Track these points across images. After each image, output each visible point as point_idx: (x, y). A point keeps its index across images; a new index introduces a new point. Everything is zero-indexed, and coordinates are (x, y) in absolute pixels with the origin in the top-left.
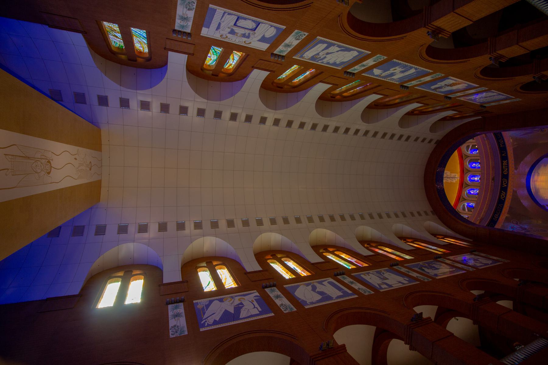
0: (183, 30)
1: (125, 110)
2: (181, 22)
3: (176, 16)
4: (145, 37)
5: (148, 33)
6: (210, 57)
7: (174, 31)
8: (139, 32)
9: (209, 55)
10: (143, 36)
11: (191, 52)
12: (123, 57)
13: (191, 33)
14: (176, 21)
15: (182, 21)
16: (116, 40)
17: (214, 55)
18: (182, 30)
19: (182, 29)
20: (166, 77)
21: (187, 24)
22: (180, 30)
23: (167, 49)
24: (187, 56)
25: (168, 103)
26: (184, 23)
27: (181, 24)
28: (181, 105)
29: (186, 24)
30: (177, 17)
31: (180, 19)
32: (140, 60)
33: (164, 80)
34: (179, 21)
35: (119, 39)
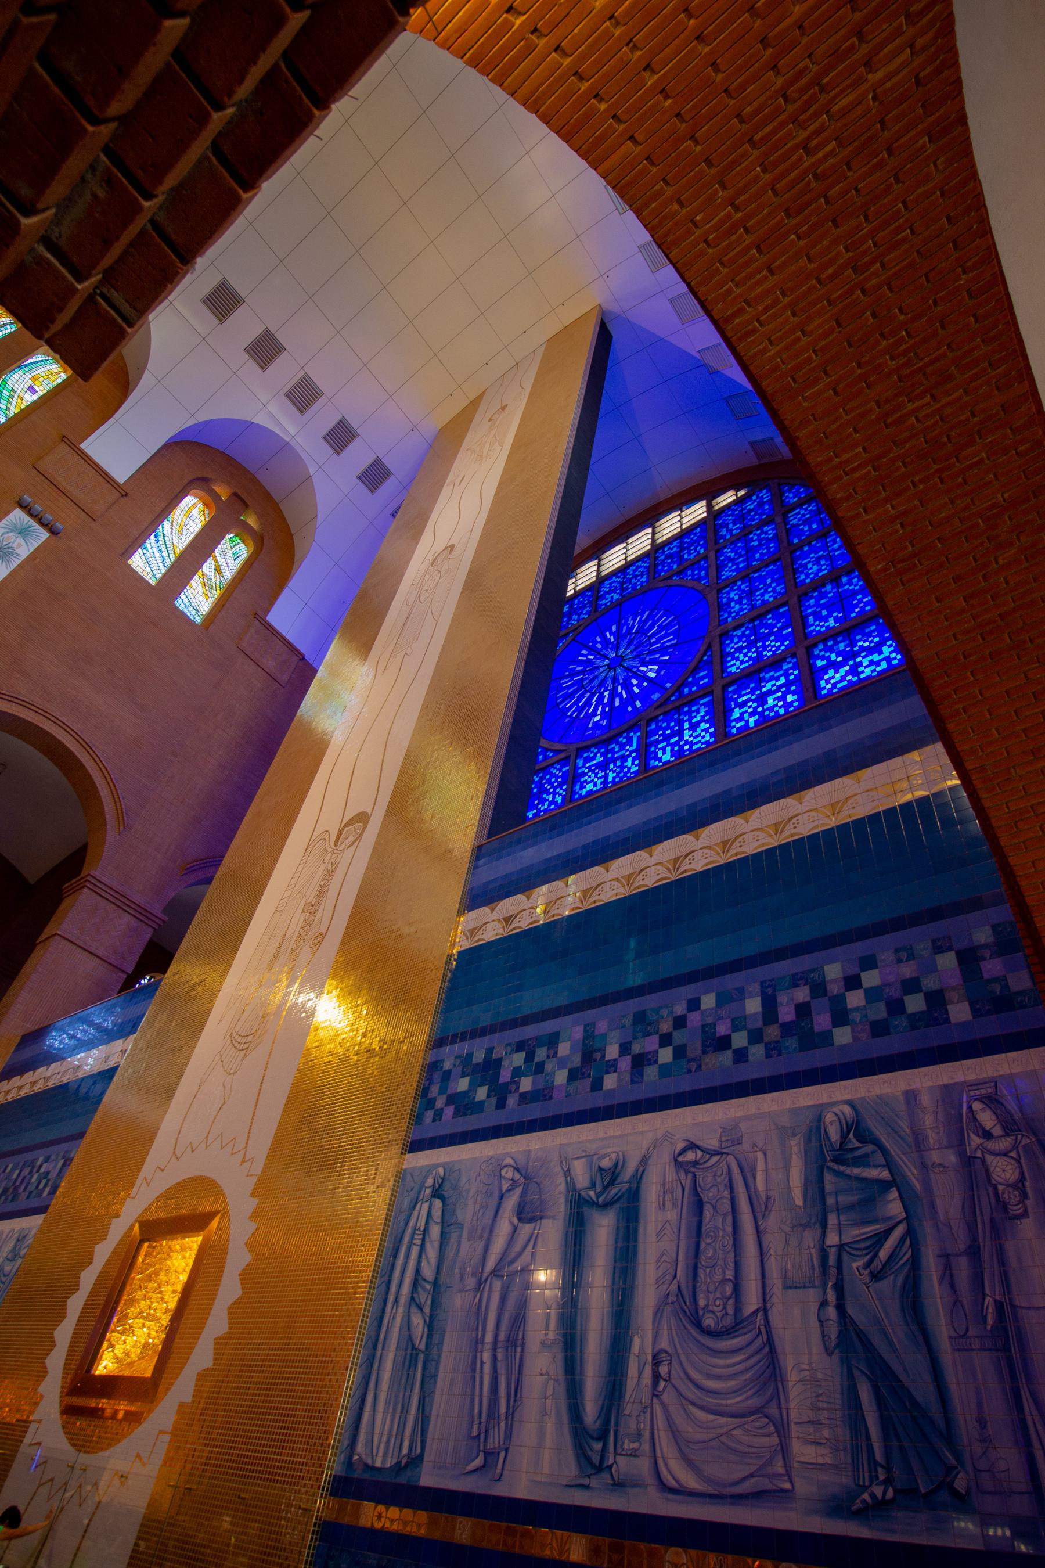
0: (32, 522)
1: (354, 423)
2: (19, 545)
3: (19, 566)
4: (156, 536)
5: (130, 552)
6: (32, 390)
7: (53, 532)
8: (157, 555)
9: (30, 398)
10: (157, 541)
11: (63, 449)
12: (252, 521)
13: (16, 505)
14: (29, 553)
15: (12, 548)
16: (229, 561)
17: (13, 390)
18: (34, 523)
19: (29, 527)
20: (192, 422)
21: (5, 536)
22: (38, 527)
23: (123, 492)
24: (83, 446)
25: (247, 356)
26: (12, 540)
27: (22, 541)
28: (217, 322)
29: (11, 534)
30: (16, 562)
31: (12, 554)
32: (223, 492)
33: (203, 417)
34: (18, 551)
35: (219, 559)
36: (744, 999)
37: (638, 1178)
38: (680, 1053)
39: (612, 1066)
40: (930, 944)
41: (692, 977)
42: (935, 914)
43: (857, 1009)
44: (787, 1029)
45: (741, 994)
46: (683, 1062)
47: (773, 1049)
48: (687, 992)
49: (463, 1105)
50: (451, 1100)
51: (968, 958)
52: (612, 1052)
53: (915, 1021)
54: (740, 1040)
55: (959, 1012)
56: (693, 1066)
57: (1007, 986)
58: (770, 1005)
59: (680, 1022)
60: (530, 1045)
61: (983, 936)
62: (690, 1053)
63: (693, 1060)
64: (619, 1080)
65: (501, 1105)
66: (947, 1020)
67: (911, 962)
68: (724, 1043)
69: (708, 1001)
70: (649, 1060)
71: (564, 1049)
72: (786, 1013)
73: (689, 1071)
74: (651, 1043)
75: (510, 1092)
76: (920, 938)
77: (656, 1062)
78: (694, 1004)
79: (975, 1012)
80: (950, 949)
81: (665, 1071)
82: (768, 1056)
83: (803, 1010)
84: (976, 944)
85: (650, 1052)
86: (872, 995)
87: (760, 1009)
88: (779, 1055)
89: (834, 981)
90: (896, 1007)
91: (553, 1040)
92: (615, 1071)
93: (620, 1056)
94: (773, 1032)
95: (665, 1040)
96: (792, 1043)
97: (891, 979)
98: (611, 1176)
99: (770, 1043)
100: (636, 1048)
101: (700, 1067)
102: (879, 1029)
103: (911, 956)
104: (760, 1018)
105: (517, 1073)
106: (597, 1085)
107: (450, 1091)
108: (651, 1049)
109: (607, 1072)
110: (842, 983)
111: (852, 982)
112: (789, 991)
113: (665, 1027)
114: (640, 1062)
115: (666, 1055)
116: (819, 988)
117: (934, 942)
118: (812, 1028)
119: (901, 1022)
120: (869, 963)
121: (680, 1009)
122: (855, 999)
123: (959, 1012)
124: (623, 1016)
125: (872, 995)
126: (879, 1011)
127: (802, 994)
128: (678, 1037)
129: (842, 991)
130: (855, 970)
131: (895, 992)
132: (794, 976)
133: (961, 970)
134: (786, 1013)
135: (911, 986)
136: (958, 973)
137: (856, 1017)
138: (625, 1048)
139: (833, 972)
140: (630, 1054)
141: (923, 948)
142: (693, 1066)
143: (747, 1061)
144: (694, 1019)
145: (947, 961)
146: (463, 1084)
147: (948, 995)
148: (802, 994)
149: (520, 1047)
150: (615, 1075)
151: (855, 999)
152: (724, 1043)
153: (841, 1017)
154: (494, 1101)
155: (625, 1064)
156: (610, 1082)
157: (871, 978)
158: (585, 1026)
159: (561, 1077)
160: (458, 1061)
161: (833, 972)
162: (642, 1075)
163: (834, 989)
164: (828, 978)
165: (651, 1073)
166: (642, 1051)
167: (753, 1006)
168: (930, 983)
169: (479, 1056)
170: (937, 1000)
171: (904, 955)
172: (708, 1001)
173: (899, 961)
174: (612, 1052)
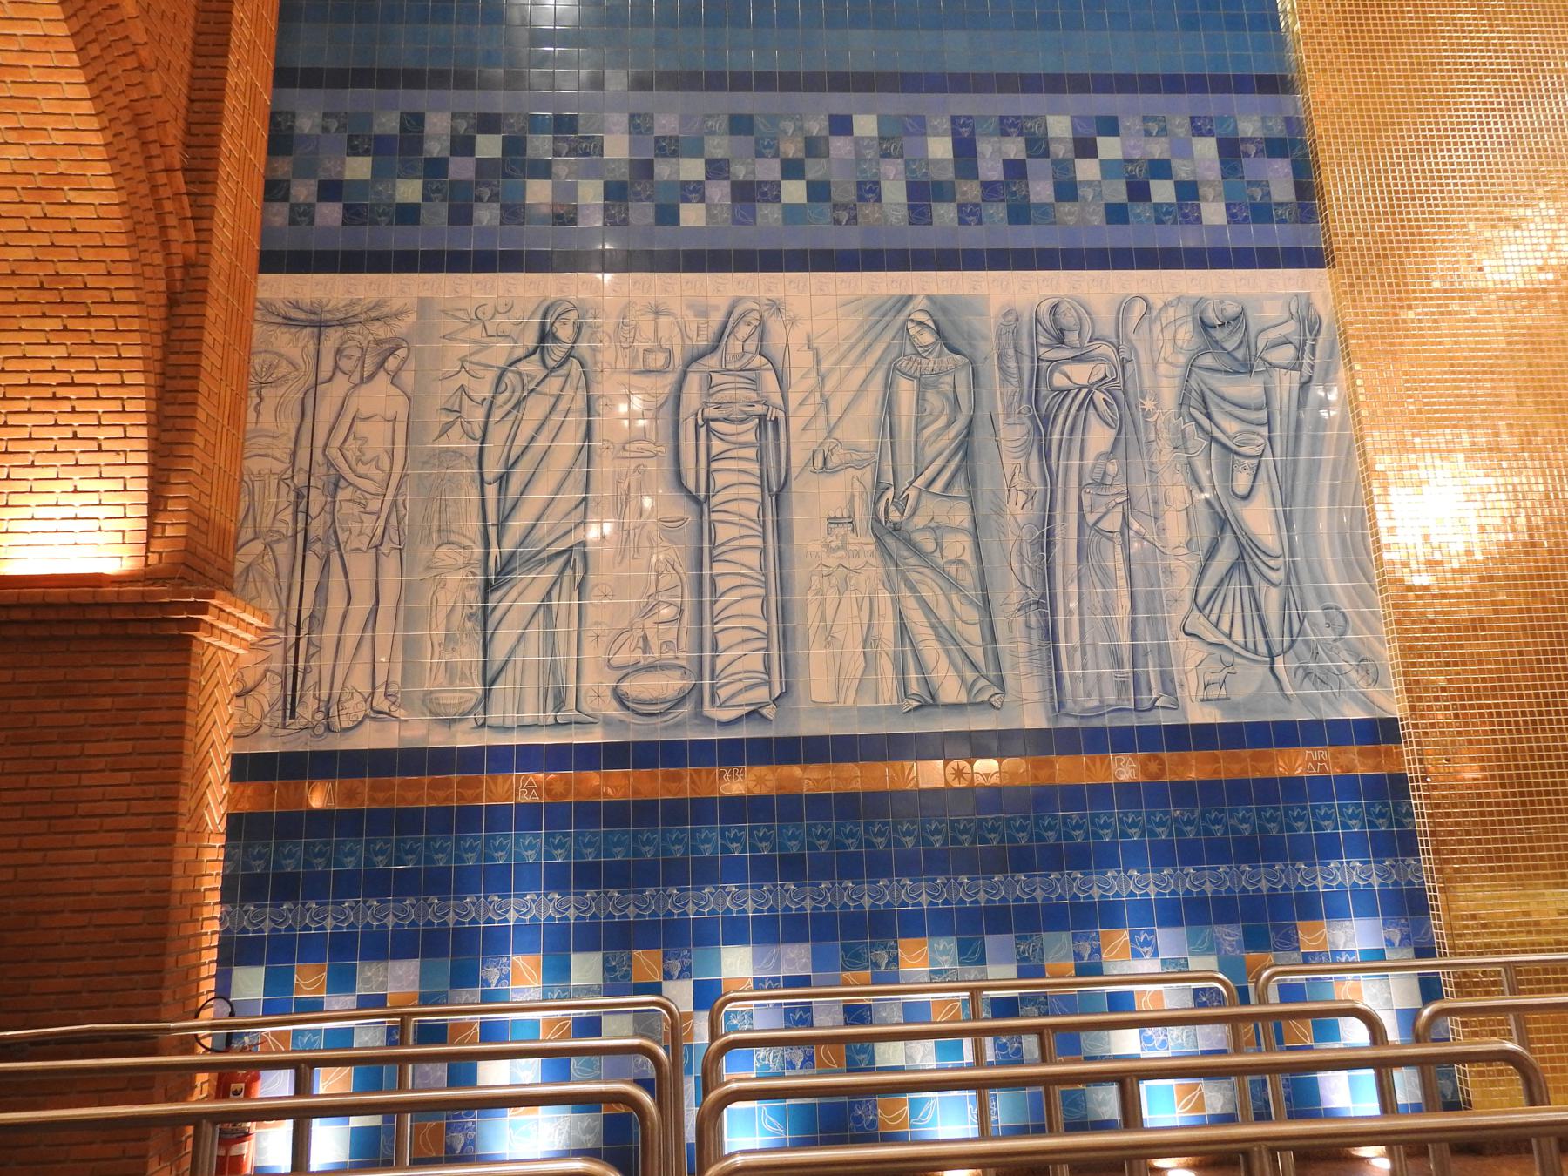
36: (925, 134)
38: (818, 191)
39: (693, 191)
40: (1188, 121)
41: (841, 82)
42: (1197, 84)
43: (1090, 184)
44: (990, 189)
45: (919, 126)
46: (826, 207)
47: (968, 214)
48: (838, 102)
50: (331, 190)
51: (1230, 150)
53: (1161, 213)
55: (1214, 212)
56: (844, 216)
57: (1269, 193)
58: (965, 150)
59: (814, 147)
60: (512, 125)
61: (1249, 127)
62: (837, 195)
63: (845, 207)
64: (709, 215)
65: (461, 215)
66: (1199, 220)
67: (1163, 139)
69: (866, 125)
70: (765, 194)
72: (991, 170)
73: (837, 222)
74: (769, 169)
75: (479, 199)
76: (1179, 109)
77: (778, 198)
78: (842, 125)
79: (1232, 217)
80: (1210, 133)
81: (792, 213)
82: (962, 221)
83: (1015, 169)
84: (1241, 135)
85: (766, 183)
86: (1108, 167)
87: (950, 155)
88: (980, 222)
89: (1060, 140)
90: (1139, 191)
92: (702, 200)
93: (707, 178)
94: (970, 191)
95: (792, 169)
96: (997, 211)
97: (1136, 154)
99: (965, 205)
100: (740, 172)
101: (853, 219)
102: (1116, 214)
103: (1163, 131)
104: (951, 167)
106: (667, 215)
107: (323, 176)
108: (771, 179)
109: (686, 200)
110: (1071, 146)
111: (1086, 148)
112: (995, 139)
113: (791, 149)
114: (748, 194)
115: (794, 192)
116: (1038, 145)
117: (1193, 119)
118: (1026, 197)
119: (1139, 210)
120: (1110, 126)
121: (817, 126)
122: (1087, 170)
123: (1214, 212)
124: (709, 116)
125: (1108, 167)
126: (1118, 192)
127: (1014, 148)
128: (815, 170)
129: (1071, 155)
130: (1087, 132)
131: (1140, 173)
132: (1002, 119)
133: (1222, 163)
134: (991, 170)
135: (1161, 169)
136: (1217, 165)
137: (1089, 194)
139: (1059, 127)
140: (727, 178)
141: (1180, 126)
142: (844, 216)
143: (931, 223)
144: (840, 146)
145: (1206, 148)
147: (1202, 191)
148: (1014, 148)
150: (702, 206)
151: (1087, 170)
153: (1067, 190)
154: (443, 209)
155: (719, 192)
156: (692, 215)
157: (1109, 147)
158: (632, 116)
160: (334, 125)
161: (1059, 127)
162: (754, 217)
163: (1061, 150)
164: (1050, 135)
165: (769, 214)
166: (750, 178)
167: (940, 148)
168: (1182, 170)
169: (388, 123)
170: (1189, 192)
171: (1154, 129)
172: (866, 125)
173: (1148, 133)
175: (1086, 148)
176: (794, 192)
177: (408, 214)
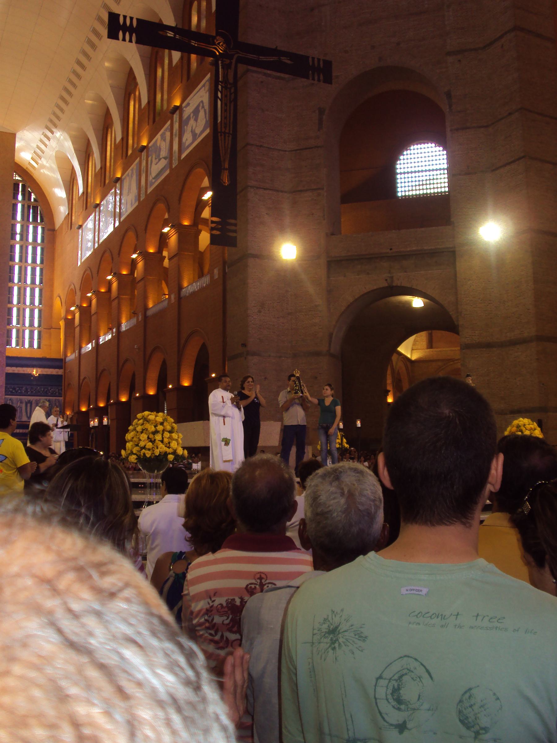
37: (32, 401)
38: (36, 392)
49: (11, 392)
50: (10, 391)
52: (29, 390)
54: (41, 392)
55: (57, 394)
59: (36, 389)
65: (16, 393)
68: (40, 392)
69: (39, 388)
71: (23, 389)
72: (45, 391)
74: (33, 390)
78: (37, 388)
91: (22, 387)
95: (34, 390)
98: (30, 401)
105: (18, 390)
106: (28, 393)
111: (51, 390)
114: (32, 392)
115: (34, 392)
123: (57, 394)
134: (45, 391)
138: (30, 390)
139: (49, 388)
144: (37, 389)
145: (57, 390)
146: (11, 390)
148: (46, 390)
149: (18, 387)
151: (51, 391)
152: (40, 392)
153: (49, 392)
155: (30, 392)
156: (29, 393)
159: (23, 391)
161: (49, 388)
167: (43, 389)
169: (13, 387)
174: (29, 390)
175: (51, 390)
176: (34, 392)
177: (13, 392)
